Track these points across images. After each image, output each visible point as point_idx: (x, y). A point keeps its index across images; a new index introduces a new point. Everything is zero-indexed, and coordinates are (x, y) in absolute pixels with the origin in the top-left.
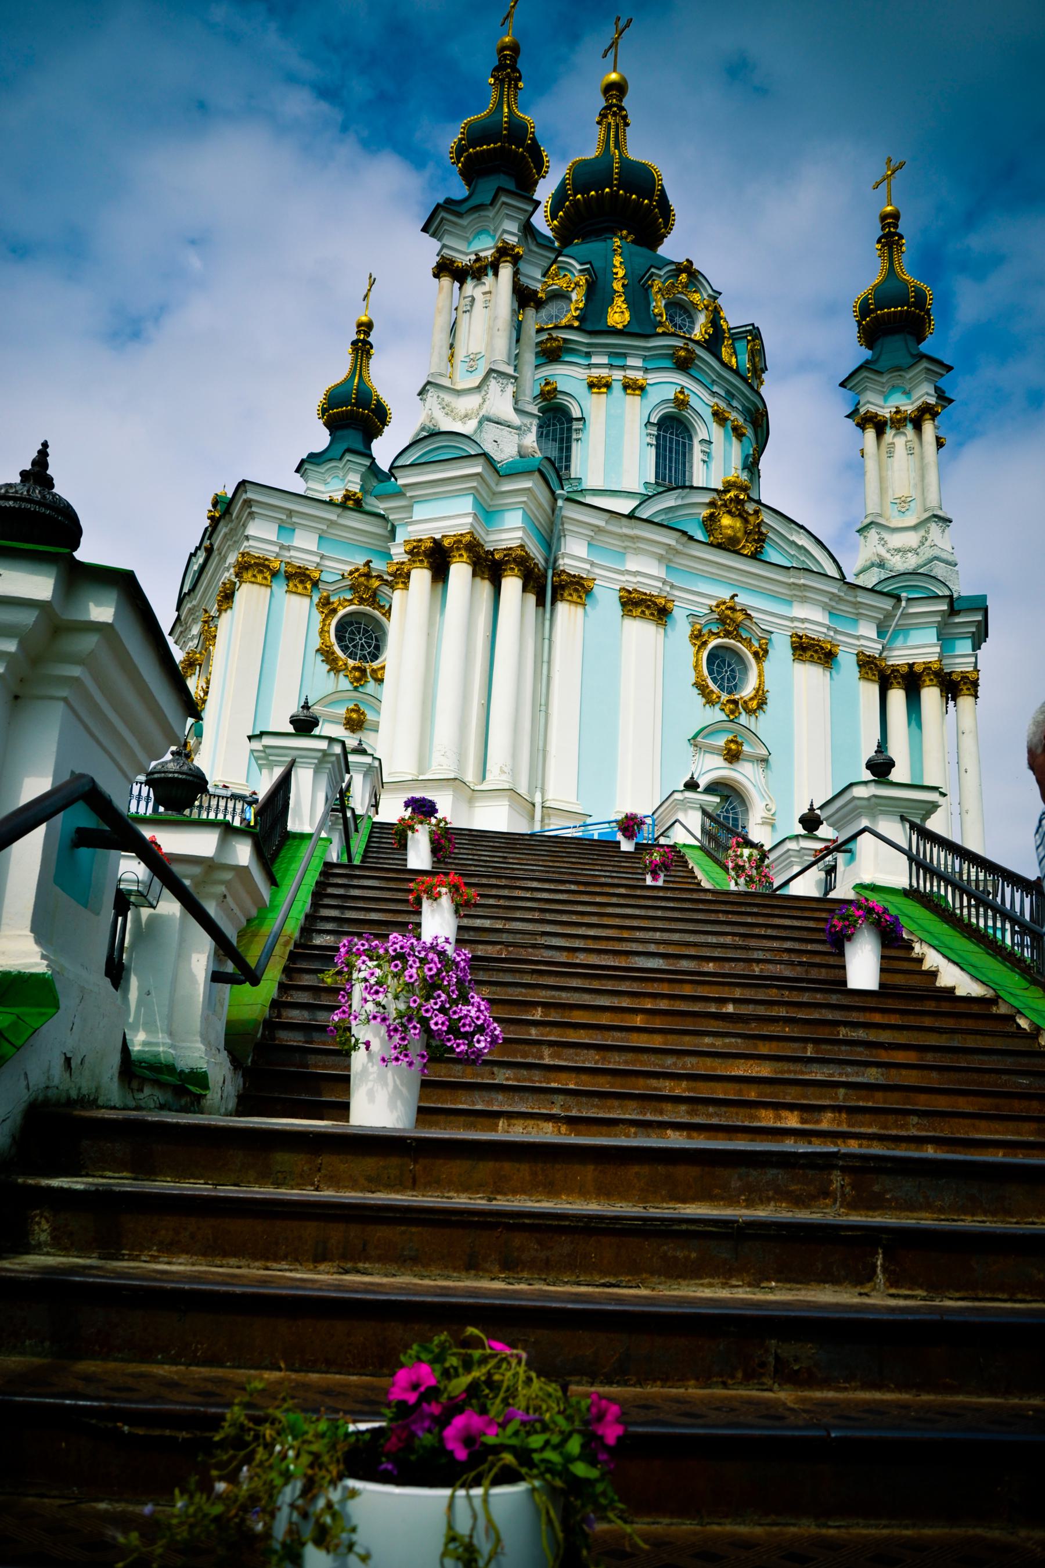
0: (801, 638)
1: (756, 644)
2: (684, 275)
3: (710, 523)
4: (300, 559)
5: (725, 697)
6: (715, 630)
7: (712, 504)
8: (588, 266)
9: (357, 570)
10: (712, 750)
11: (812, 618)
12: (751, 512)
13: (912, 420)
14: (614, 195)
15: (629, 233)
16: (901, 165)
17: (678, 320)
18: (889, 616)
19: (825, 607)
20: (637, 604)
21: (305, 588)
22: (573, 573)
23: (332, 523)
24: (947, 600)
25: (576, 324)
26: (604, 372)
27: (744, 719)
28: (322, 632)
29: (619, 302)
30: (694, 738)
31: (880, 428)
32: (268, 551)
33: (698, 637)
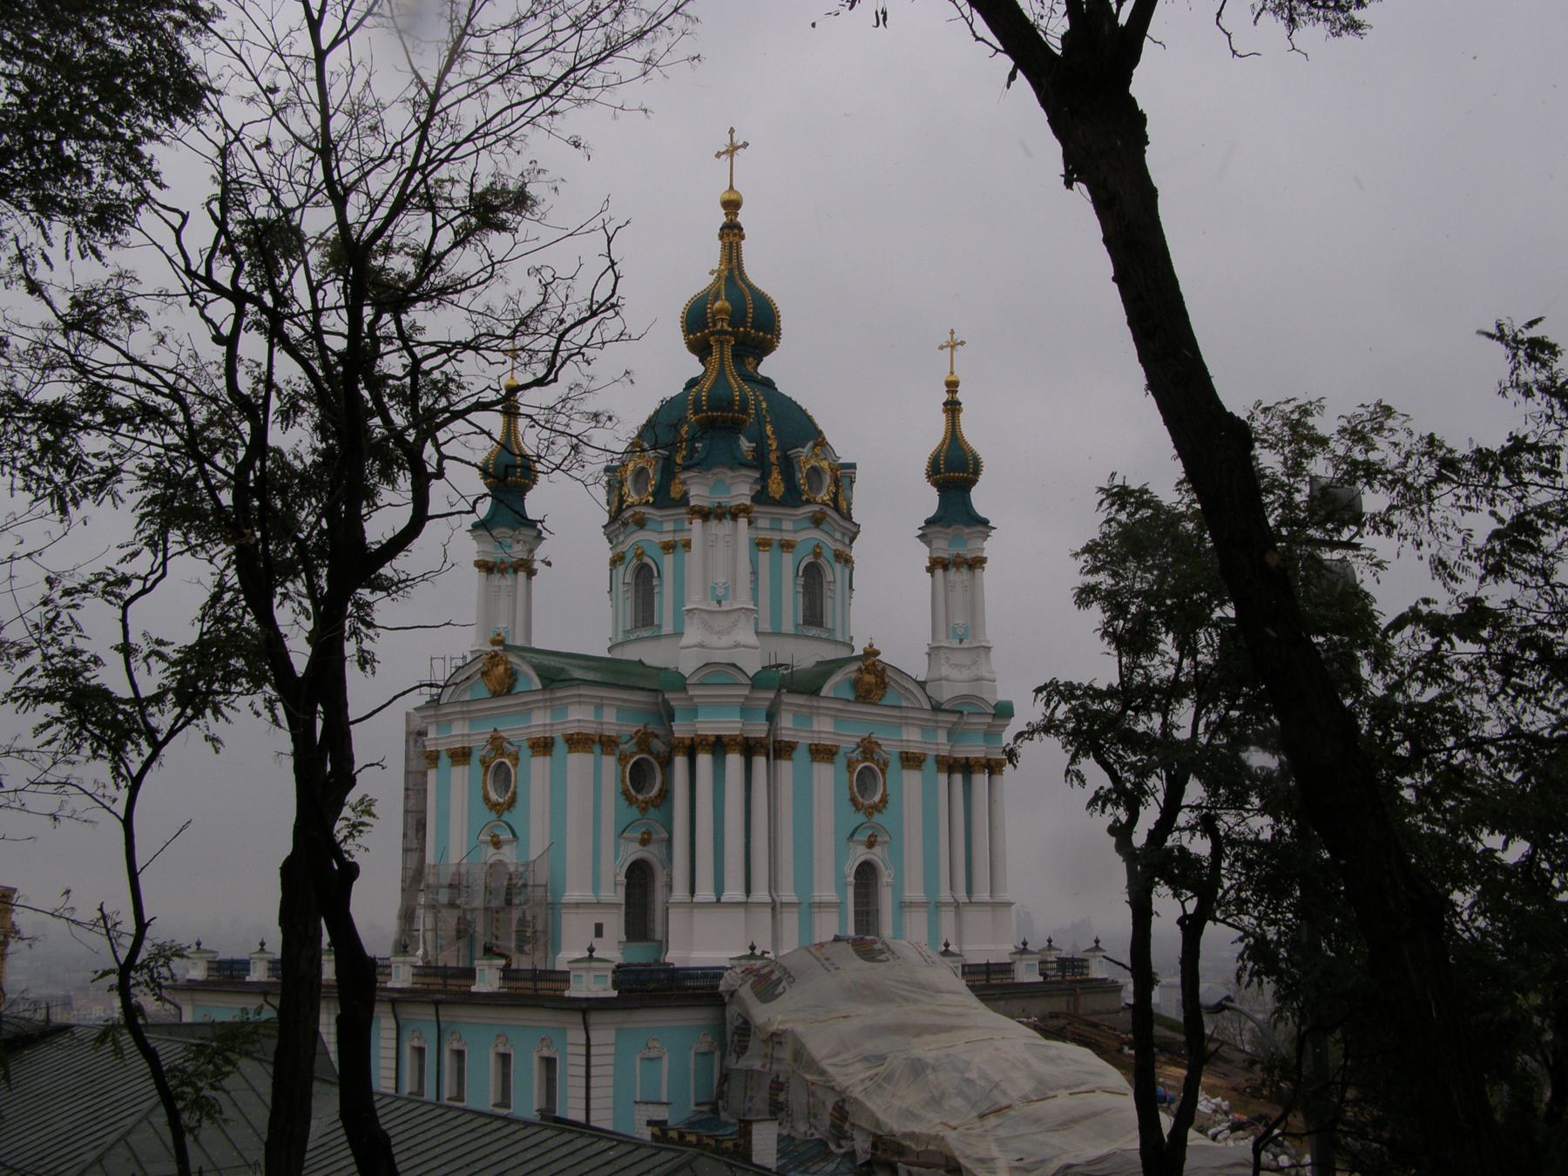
2: (818, 450)
3: (856, 684)
4: (610, 731)
7: (859, 670)
10: (859, 842)
11: (912, 738)
14: (747, 334)
16: (962, 343)
18: (955, 724)
19: (920, 726)
23: (625, 700)
26: (767, 535)
27: (876, 815)
28: (623, 781)
29: (776, 475)
30: (852, 835)
31: (945, 568)
32: (590, 729)
33: (850, 766)
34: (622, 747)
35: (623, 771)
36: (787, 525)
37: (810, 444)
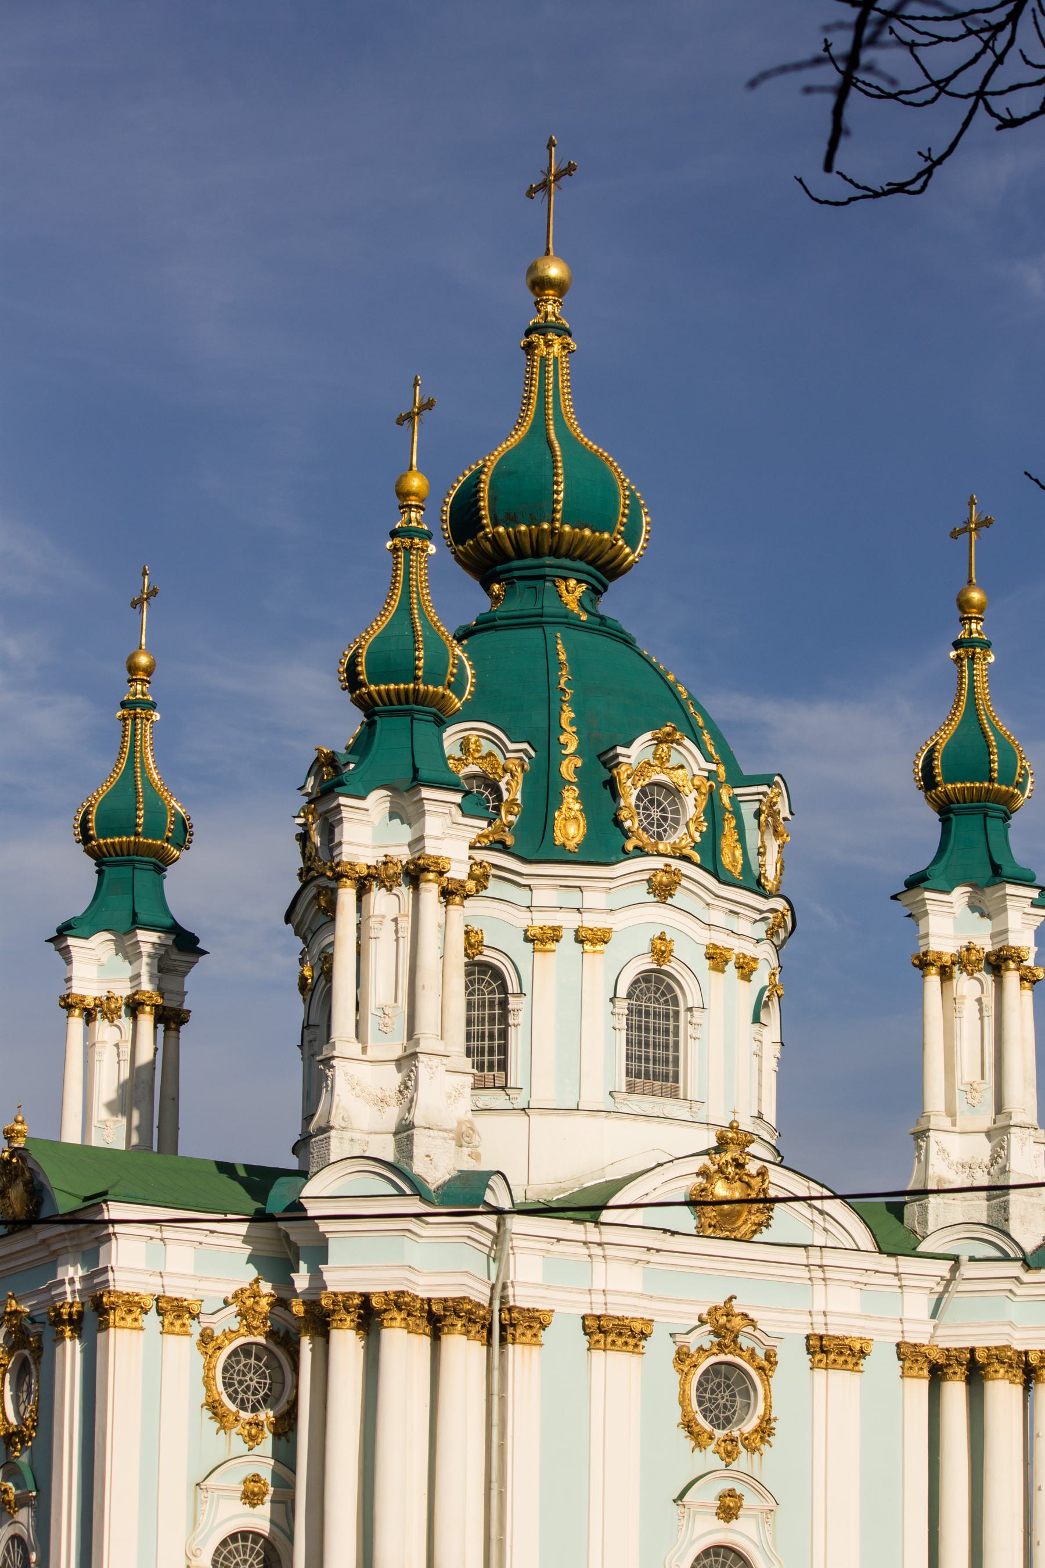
0: (821, 1337)
1: (760, 1353)
2: (664, 746)
5: (720, 1434)
6: (707, 1346)
7: (703, 1173)
8: (525, 746)
9: (243, 1291)
12: (754, 1172)
13: (988, 962)
15: (579, 581)
17: (656, 813)
20: (606, 1331)
21: (184, 1325)
22: (525, 1306)
24: (1020, 1263)
25: (509, 841)
27: (743, 1461)
29: (571, 802)
34: (202, 1318)
35: (208, 1368)
36: (593, 899)
37: (648, 735)
